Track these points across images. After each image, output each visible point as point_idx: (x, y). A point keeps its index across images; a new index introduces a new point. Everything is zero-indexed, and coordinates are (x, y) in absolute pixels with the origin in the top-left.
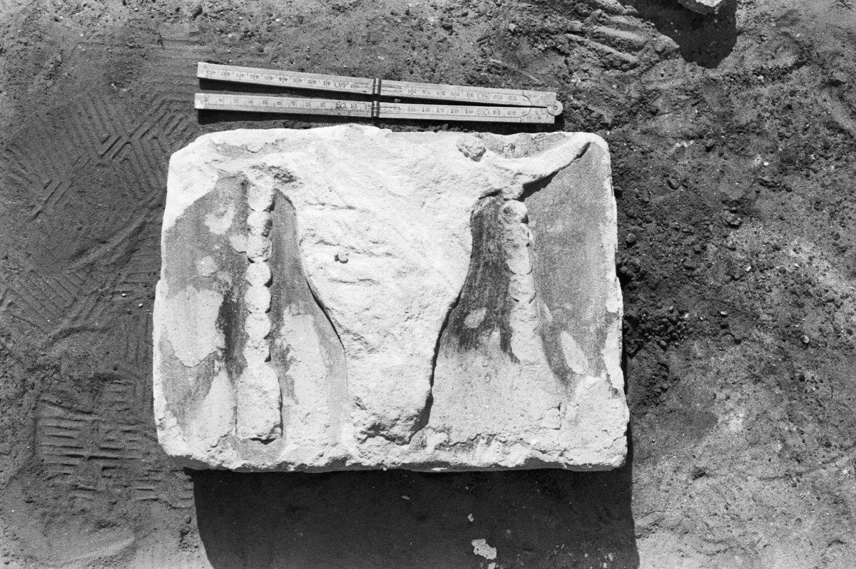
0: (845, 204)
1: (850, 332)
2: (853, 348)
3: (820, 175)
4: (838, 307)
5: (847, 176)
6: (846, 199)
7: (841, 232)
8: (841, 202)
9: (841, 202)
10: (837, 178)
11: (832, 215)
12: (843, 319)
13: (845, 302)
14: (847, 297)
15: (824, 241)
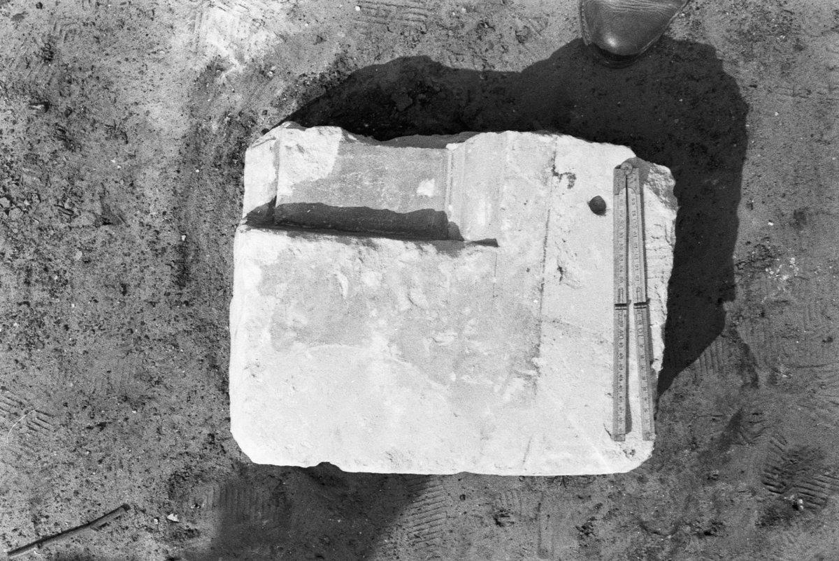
0: (79, 246)
1: (164, 213)
2: (175, 208)
3: (65, 268)
4: (150, 226)
5: (59, 250)
6: (76, 246)
7: (99, 240)
8: (79, 248)
9: (79, 248)
10: (64, 257)
11: (90, 251)
12: (158, 220)
13: (145, 222)
14: (142, 223)
15: (110, 250)
